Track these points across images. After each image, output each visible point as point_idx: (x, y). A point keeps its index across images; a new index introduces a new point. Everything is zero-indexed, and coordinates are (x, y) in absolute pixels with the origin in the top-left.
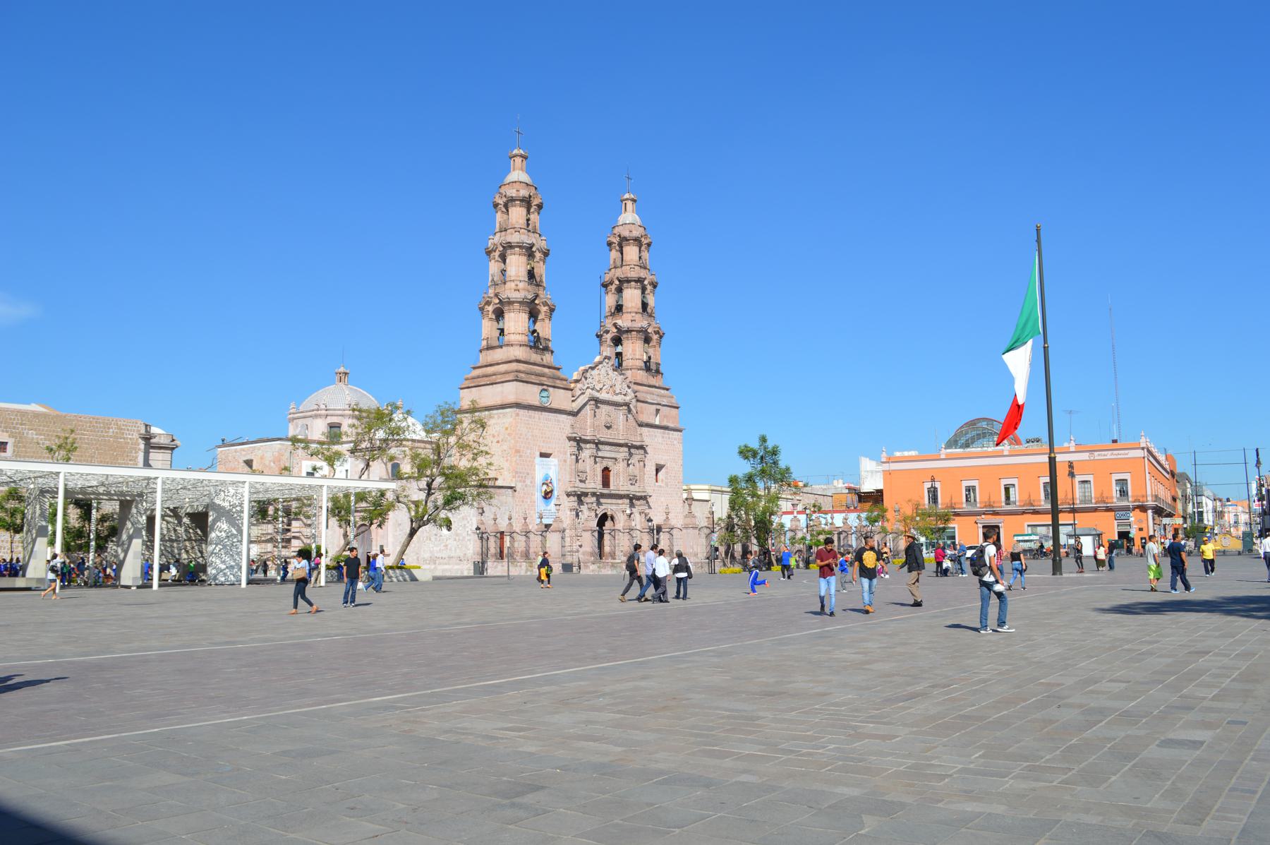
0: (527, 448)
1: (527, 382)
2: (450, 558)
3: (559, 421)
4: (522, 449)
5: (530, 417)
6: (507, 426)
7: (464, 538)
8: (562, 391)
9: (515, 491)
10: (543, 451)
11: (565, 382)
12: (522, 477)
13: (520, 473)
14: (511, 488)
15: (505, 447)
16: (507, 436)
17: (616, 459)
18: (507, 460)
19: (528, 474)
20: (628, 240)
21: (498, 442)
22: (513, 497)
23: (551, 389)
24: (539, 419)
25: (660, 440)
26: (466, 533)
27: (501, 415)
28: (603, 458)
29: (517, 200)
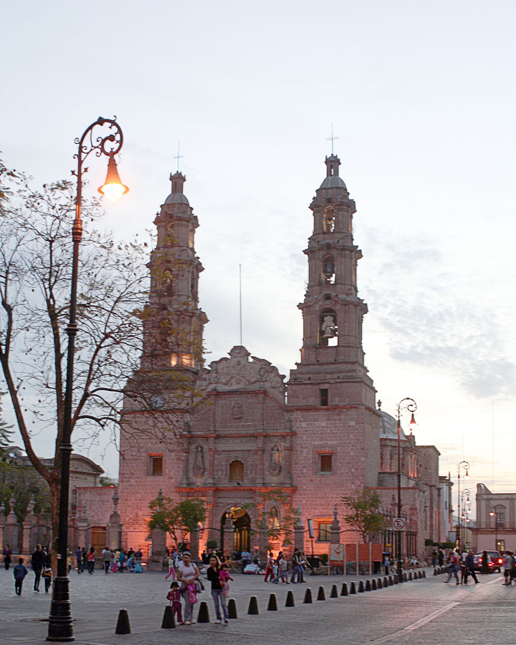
10: (150, 452)
13: (123, 474)
17: (249, 451)
19: (132, 474)
25: (324, 424)
28: (229, 451)
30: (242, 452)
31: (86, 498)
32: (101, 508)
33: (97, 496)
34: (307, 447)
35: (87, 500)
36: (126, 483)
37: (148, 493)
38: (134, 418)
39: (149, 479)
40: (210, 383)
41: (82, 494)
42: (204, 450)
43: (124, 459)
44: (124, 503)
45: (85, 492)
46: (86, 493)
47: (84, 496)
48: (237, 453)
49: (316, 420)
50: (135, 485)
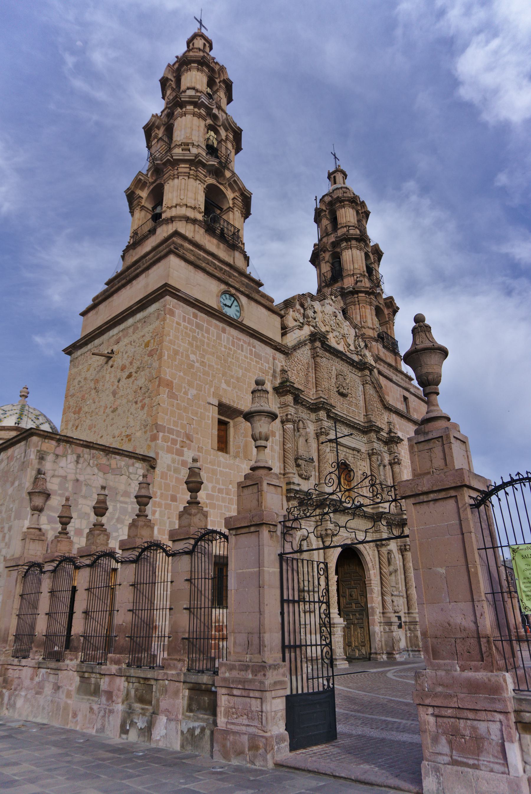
0: (190, 384)
1: (197, 267)
4: (174, 381)
5: (198, 326)
6: (147, 339)
8: (264, 310)
9: (154, 468)
10: (225, 401)
12: (174, 442)
13: (171, 431)
14: (144, 459)
15: (141, 382)
16: (147, 358)
18: (143, 407)
19: (189, 437)
20: (343, 201)
21: (129, 376)
23: (244, 300)
24: (219, 337)
27: (139, 325)
30: (351, 452)
31: (61, 472)
33: (96, 470)
36: (174, 456)
37: (220, 491)
38: (195, 316)
39: (222, 459)
41: (50, 458)
42: (308, 430)
44: (168, 506)
45: (60, 450)
46: (65, 455)
48: (345, 449)
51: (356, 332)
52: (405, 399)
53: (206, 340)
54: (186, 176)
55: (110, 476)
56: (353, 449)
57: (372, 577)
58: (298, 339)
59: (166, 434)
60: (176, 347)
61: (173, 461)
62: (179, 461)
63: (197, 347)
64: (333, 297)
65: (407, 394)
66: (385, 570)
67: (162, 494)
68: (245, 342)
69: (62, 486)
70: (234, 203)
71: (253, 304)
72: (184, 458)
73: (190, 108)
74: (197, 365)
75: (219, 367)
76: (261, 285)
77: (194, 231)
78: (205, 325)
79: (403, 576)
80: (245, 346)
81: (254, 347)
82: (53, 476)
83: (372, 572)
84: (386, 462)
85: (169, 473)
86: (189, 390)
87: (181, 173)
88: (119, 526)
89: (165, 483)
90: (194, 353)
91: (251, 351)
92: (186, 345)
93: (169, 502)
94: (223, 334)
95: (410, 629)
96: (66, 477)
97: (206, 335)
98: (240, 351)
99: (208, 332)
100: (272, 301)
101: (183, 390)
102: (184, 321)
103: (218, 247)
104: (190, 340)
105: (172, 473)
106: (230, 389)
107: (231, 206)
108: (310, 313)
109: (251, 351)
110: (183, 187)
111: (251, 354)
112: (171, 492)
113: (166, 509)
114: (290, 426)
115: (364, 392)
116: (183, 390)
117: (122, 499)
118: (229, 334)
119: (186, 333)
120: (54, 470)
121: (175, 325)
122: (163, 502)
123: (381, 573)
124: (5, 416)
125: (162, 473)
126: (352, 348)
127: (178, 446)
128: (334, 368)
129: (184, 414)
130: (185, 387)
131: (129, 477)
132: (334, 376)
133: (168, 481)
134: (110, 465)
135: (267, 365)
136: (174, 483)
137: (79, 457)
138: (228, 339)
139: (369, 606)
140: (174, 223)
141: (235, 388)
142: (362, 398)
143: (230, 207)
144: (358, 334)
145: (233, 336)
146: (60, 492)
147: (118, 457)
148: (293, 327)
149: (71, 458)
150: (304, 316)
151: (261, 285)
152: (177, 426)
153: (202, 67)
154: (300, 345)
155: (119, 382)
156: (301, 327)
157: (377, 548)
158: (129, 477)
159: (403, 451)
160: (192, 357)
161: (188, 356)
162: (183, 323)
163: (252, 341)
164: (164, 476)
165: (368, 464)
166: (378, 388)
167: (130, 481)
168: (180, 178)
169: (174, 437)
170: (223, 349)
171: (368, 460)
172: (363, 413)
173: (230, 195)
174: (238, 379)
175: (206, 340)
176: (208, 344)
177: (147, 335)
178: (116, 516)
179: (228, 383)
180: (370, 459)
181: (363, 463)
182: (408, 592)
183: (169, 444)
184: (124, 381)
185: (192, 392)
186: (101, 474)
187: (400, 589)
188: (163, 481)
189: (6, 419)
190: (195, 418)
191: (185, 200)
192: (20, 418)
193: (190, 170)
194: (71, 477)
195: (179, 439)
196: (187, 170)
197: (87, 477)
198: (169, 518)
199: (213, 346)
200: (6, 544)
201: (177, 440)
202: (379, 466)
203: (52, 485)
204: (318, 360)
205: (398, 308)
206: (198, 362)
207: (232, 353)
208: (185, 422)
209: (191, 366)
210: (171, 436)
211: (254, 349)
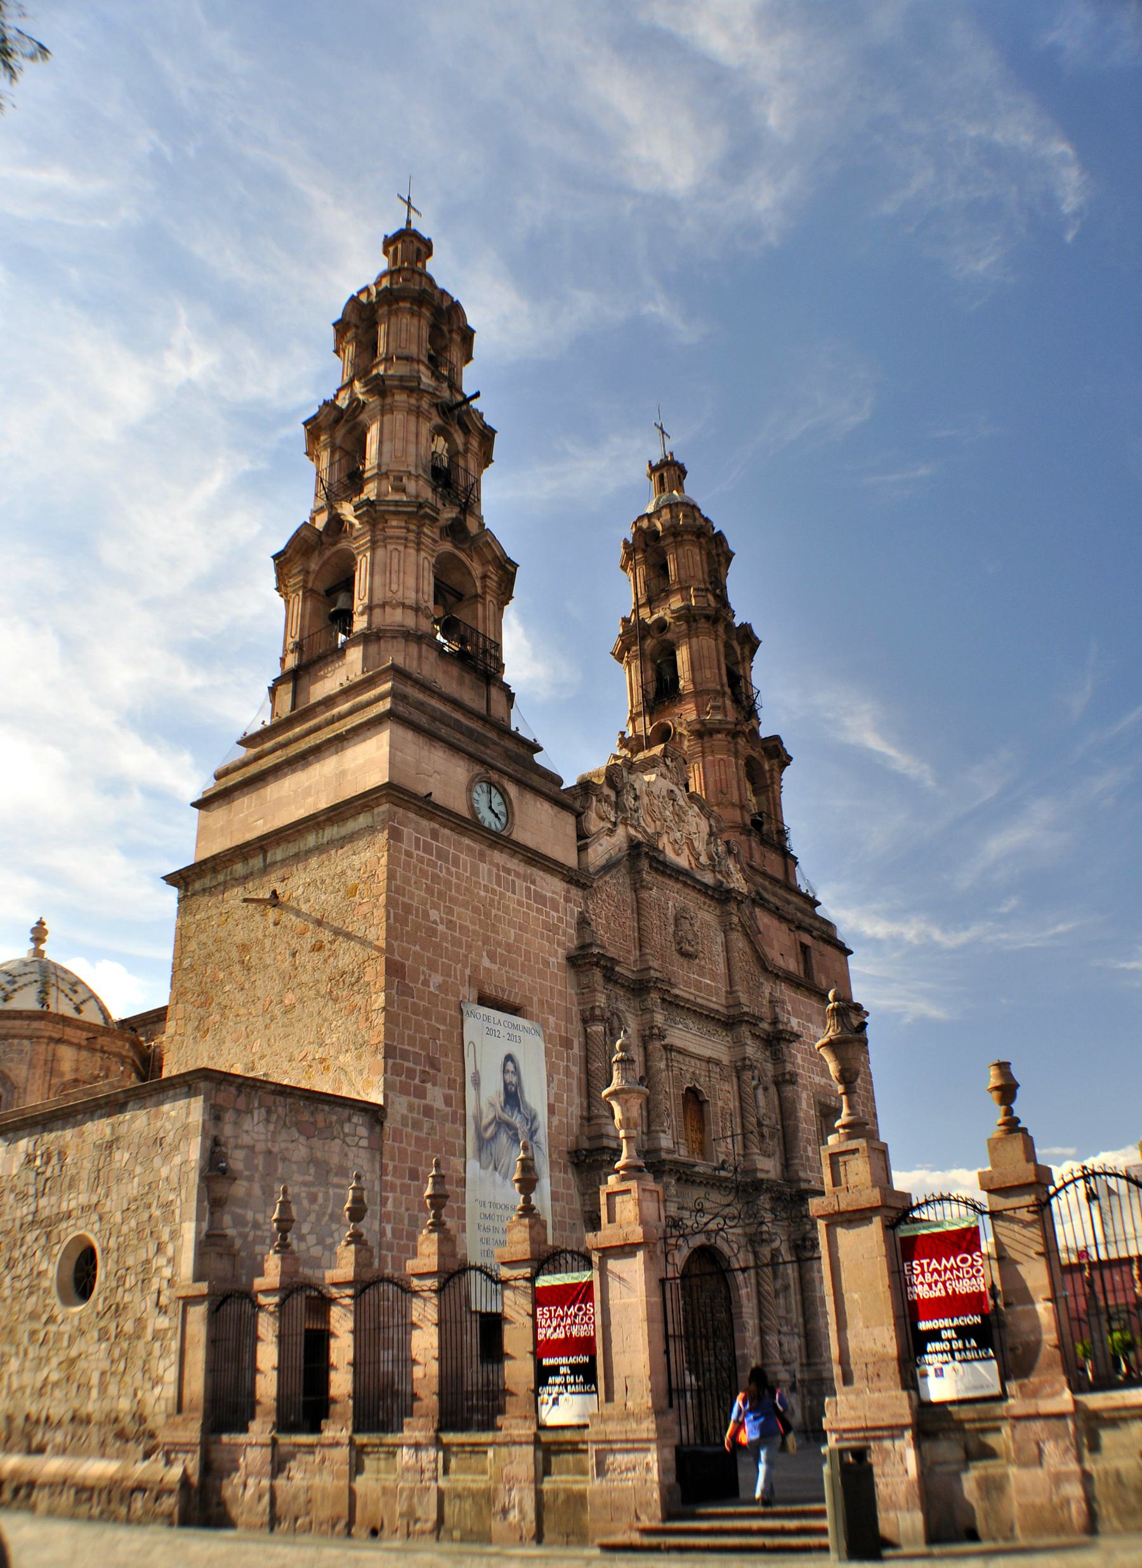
0: (432, 966)
2: (79, 1420)
3: (540, 898)
5: (442, 855)
7: (140, 1322)
10: (489, 990)
11: (551, 785)
12: (411, 1073)
13: (405, 1055)
19: (433, 1063)
22: (376, 1147)
23: (512, 790)
26: (150, 1300)
29: (404, 299)
31: (246, 1140)
32: (313, 1199)
34: (805, 1087)
35: (251, 1148)
38: (435, 835)
40: (625, 822)
41: (229, 1116)
43: (405, 991)
44: (405, 1189)
45: (241, 1102)
46: (250, 1111)
47: (236, 1124)
48: (693, 1061)
49: (810, 1020)
50: (444, 1118)
51: (710, 826)
52: (805, 949)
53: (454, 880)
54: (400, 544)
55: (315, 1142)
56: (709, 1060)
57: (744, 1301)
58: (607, 856)
59: (398, 1061)
60: (406, 900)
61: (411, 1108)
62: (419, 1106)
63: (440, 893)
64: (668, 761)
65: (807, 939)
66: (767, 1288)
67: (395, 1167)
68: (517, 875)
69: (248, 1161)
70: (484, 587)
71: (529, 797)
72: (427, 1102)
73: (400, 398)
74: (441, 928)
75: (477, 928)
76: (538, 749)
77: (420, 657)
78: (452, 851)
79: (799, 1297)
80: (518, 881)
81: (533, 882)
82: (237, 1147)
83: (743, 1292)
84: (768, 1079)
85: (405, 1130)
86: (430, 976)
87: (391, 538)
88: (334, 1226)
89: (399, 1148)
90: (435, 906)
91: (528, 889)
92: (423, 894)
93: (407, 1181)
94: (481, 865)
95: (810, 1393)
96: (254, 1146)
97: (454, 869)
98: (509, 894)
99: (456, 863)
100: (558, 781)
101: (422, 977)
102: (417, 848)
103: (461, 682)
104: (429, 882)
105: (409, 1130)
106: (495, 967)
107: (479, 591)
108: (630, 802)
109: (528, 889)
110: (395, 567)
111: (529, 897)
112: (409, 1164)
113: (402, 1193)
114: (599, 1028)
115: (727, 947)
116: (422, 977)
117: (336, 1180)
118: (491, 863)
119: (421, 870)
120: (236, 1137)
121: (403, 857)
122: (398, 1182)
123: (759, 1293)
124: (16, 986)
125: (395, 1130)
126: (704, 859)
127: (417, 1081)
128: (670, 904)
129: (425, 1022)
130: (423, 973)
131: (344, 1142)
132: (672, 921)
133: (404, 1145)
134: (314, 1123)
135: (555, 914)
136: (413, 1148)
137: (269, 1112)
138: (490, 871)
139: (738, 1353)
140: (382, 642)
141: (503, 964)
142: (721, 959)
143: (477, 596)
144: (715, 829)
145: (497, 866)
146: (246, 1173)
147: (326, 1108)
148: (598, 833)
149: (258, 1114)
150: (618, 806)
151: (538, 749)
152: (414, 1045)
153: (420, 307)
154: (609, 867)
155: (294, 955)
156: (611, 832)
157: (753, 1247)
158: (344, 1142)
159: (799, 1056)
160: (434, 915)
161: (426, 915)
162: (415, 852)
163: (530, 870)
164: (397, 1135)
165: (735, 1088)
166: (751, 935)
167: (347, 1149)
168: (390, 547)
169: (411, 1065)
170: (482, 893)
171: (735, 1079)
172: (723, 988)
173: (476, 569)
174: (508, 947)
175: (454, 880)
176: (458, 890)
177: (349, 872)
178: (329, 1211)
179: (492, 957)
180: (739, 1078)
181: (727, 1087)
182: (809, 1326)
183: (403, 1078)
184: (303, 958)
185: (436, 979)
186: (302, 1139)
187: (794, 1321)
188: (396, 1145)
189: (16, 995)
190: (442, 1027)
191: (400, 594)
192: (44, 992)
193: (409, 531)
194: (260, 1147)
195: (418, 1068)
196: (401, 532)
197: (283, 1145)
198: (407, 1209)
199: (467, 889)
200: (169, 1261)
201: (415, 1071)
202: (755, 1088)
203: (237, 1161)
204: (644, 894)
205: (790, 759)
206: (442, 923)
207: (497, 898)
208: (426, 1036)
209: (432, 932)
210: (406, 1064)
211: (533, 887)
